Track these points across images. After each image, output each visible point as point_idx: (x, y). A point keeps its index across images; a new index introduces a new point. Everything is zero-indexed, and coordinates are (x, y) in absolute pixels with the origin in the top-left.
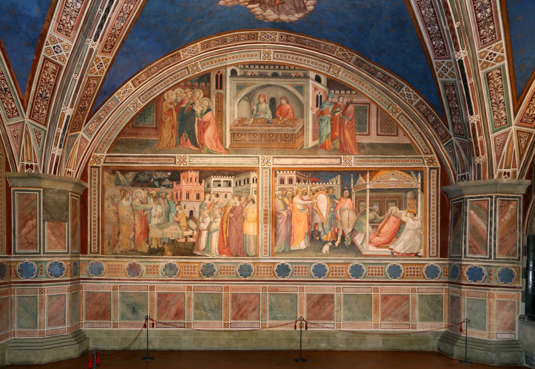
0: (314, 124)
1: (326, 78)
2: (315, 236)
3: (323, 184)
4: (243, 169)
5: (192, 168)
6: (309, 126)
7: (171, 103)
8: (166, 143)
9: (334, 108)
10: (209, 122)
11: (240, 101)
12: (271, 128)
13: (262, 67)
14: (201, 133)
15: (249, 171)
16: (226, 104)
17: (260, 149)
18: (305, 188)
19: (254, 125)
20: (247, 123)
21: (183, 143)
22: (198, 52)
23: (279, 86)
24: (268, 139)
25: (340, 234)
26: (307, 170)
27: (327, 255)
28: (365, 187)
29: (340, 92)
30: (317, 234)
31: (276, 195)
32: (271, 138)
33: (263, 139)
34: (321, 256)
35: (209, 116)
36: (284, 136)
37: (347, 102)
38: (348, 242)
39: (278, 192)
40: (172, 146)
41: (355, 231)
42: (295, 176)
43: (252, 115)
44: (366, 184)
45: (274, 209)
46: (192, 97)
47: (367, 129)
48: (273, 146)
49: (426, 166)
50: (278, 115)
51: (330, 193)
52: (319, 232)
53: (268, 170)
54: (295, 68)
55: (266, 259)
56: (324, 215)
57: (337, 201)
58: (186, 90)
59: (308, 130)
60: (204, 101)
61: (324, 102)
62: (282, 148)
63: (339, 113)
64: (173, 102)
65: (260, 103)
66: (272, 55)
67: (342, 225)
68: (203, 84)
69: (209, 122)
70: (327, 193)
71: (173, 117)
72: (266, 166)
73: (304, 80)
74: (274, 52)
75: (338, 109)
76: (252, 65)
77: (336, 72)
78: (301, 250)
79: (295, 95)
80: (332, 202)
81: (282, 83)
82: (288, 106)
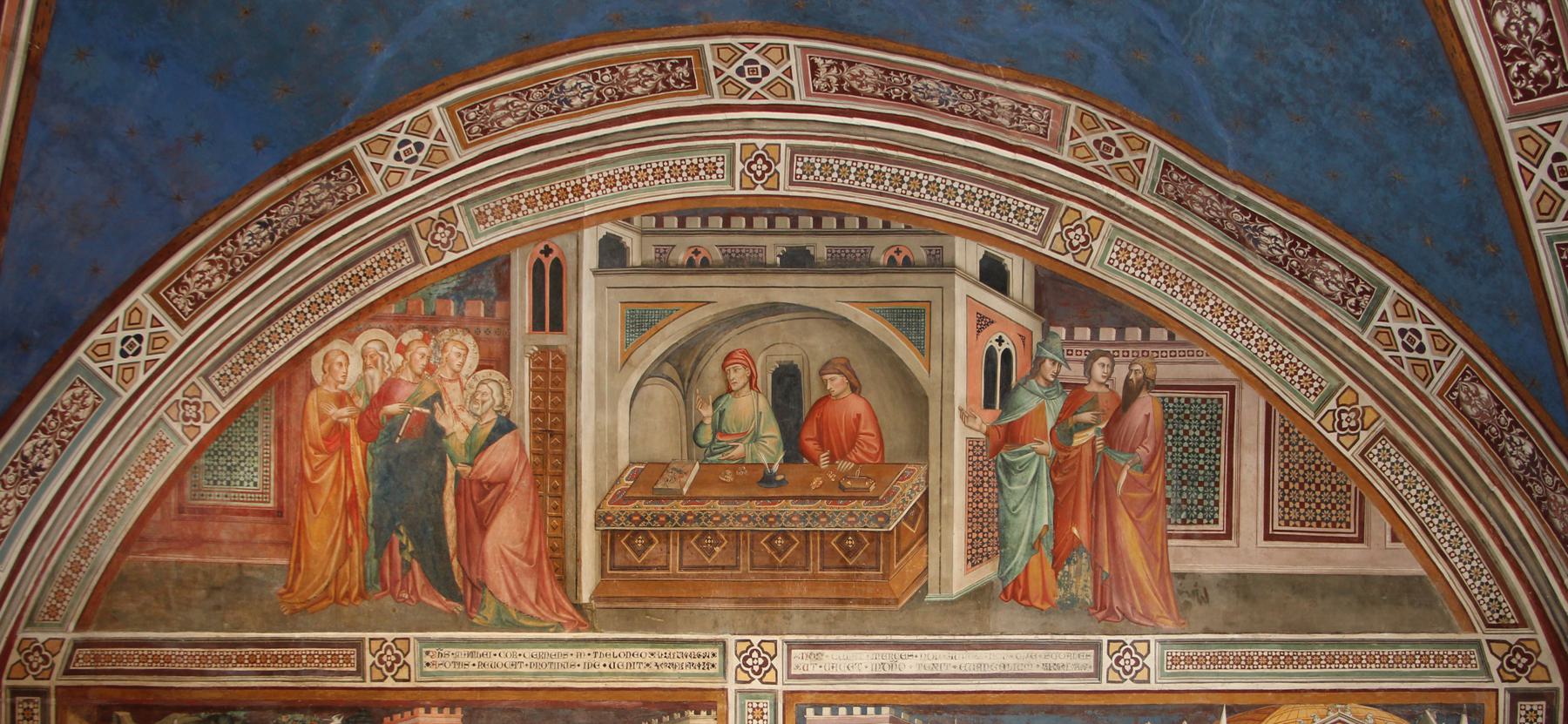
0: (975, 486)
1: (1030, 269)
4: (653, 698)
5: (432, 696)
6: (951, 495)
7: (341, 400)
8: (323, 577)
9: (1069, 409)
10: (506, 482)
11: (639, 386)
12: (776, 507)
13: (739, 223)
14: (468, 532)
15: (683, 707)
16: (577, 396)
17: (732, 606)
19: (703, 492)
20: (672, 486)
21: (394, 582)
22: (447, 158)
23: (818, 310)
24: (766, 561)
29: (1095, 335)
32: (780, 555)
33: (745, 559)
35: (502, 456)
36: (840, 543)
37: (1127, 380)
40: (348, 595)
43: (695, 450)
46: (430, 368)
47: (1222, 509)
48: (789, 591)
50: (811, 446)
53: (765, 704)
54: (886, 224)
58: (406, 339)
59: (946, 514)
60: (484, 388)
61: (1023, 383)
62: (828, 601)
63: (1091, 433)
64: (345, 393)
65: (730, 391)
66: (781, 168)
68: (477, 309)
69: (502, 484)
71: (349, 464)
72: (756, 685)
73: (928, 279)
74: (794, 150)
75: (1086, 417)
76: (695, 213)
77: (1077, 237)
79: (889, 350)
81: (831, 295)
82: (856, 405)
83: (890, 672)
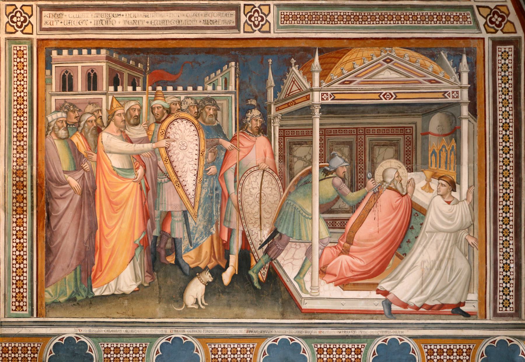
2: (163, 253)
3: (185, 89)
18: (132, 103)
25: (236, 246)
26: (139, 45)
27: (198, 310)
28: (308, 98)
30: (169, 246)
31: (49, 126)
34: (180, 314)
38: (259, 271)
39: (54, 116)
41: (281, 235)
42: (104, 65)
44: (312, 90)
45: (43, 169)
49: (484, 35)
51: (207, 120)
52: (174, 239)
55: (20, 325)
56: (190, 187)
57: (227, 145)
67: (241, 218)
70: (197, 118)
78: (124, 295)
80: (215, 147)
83: (106, 26)
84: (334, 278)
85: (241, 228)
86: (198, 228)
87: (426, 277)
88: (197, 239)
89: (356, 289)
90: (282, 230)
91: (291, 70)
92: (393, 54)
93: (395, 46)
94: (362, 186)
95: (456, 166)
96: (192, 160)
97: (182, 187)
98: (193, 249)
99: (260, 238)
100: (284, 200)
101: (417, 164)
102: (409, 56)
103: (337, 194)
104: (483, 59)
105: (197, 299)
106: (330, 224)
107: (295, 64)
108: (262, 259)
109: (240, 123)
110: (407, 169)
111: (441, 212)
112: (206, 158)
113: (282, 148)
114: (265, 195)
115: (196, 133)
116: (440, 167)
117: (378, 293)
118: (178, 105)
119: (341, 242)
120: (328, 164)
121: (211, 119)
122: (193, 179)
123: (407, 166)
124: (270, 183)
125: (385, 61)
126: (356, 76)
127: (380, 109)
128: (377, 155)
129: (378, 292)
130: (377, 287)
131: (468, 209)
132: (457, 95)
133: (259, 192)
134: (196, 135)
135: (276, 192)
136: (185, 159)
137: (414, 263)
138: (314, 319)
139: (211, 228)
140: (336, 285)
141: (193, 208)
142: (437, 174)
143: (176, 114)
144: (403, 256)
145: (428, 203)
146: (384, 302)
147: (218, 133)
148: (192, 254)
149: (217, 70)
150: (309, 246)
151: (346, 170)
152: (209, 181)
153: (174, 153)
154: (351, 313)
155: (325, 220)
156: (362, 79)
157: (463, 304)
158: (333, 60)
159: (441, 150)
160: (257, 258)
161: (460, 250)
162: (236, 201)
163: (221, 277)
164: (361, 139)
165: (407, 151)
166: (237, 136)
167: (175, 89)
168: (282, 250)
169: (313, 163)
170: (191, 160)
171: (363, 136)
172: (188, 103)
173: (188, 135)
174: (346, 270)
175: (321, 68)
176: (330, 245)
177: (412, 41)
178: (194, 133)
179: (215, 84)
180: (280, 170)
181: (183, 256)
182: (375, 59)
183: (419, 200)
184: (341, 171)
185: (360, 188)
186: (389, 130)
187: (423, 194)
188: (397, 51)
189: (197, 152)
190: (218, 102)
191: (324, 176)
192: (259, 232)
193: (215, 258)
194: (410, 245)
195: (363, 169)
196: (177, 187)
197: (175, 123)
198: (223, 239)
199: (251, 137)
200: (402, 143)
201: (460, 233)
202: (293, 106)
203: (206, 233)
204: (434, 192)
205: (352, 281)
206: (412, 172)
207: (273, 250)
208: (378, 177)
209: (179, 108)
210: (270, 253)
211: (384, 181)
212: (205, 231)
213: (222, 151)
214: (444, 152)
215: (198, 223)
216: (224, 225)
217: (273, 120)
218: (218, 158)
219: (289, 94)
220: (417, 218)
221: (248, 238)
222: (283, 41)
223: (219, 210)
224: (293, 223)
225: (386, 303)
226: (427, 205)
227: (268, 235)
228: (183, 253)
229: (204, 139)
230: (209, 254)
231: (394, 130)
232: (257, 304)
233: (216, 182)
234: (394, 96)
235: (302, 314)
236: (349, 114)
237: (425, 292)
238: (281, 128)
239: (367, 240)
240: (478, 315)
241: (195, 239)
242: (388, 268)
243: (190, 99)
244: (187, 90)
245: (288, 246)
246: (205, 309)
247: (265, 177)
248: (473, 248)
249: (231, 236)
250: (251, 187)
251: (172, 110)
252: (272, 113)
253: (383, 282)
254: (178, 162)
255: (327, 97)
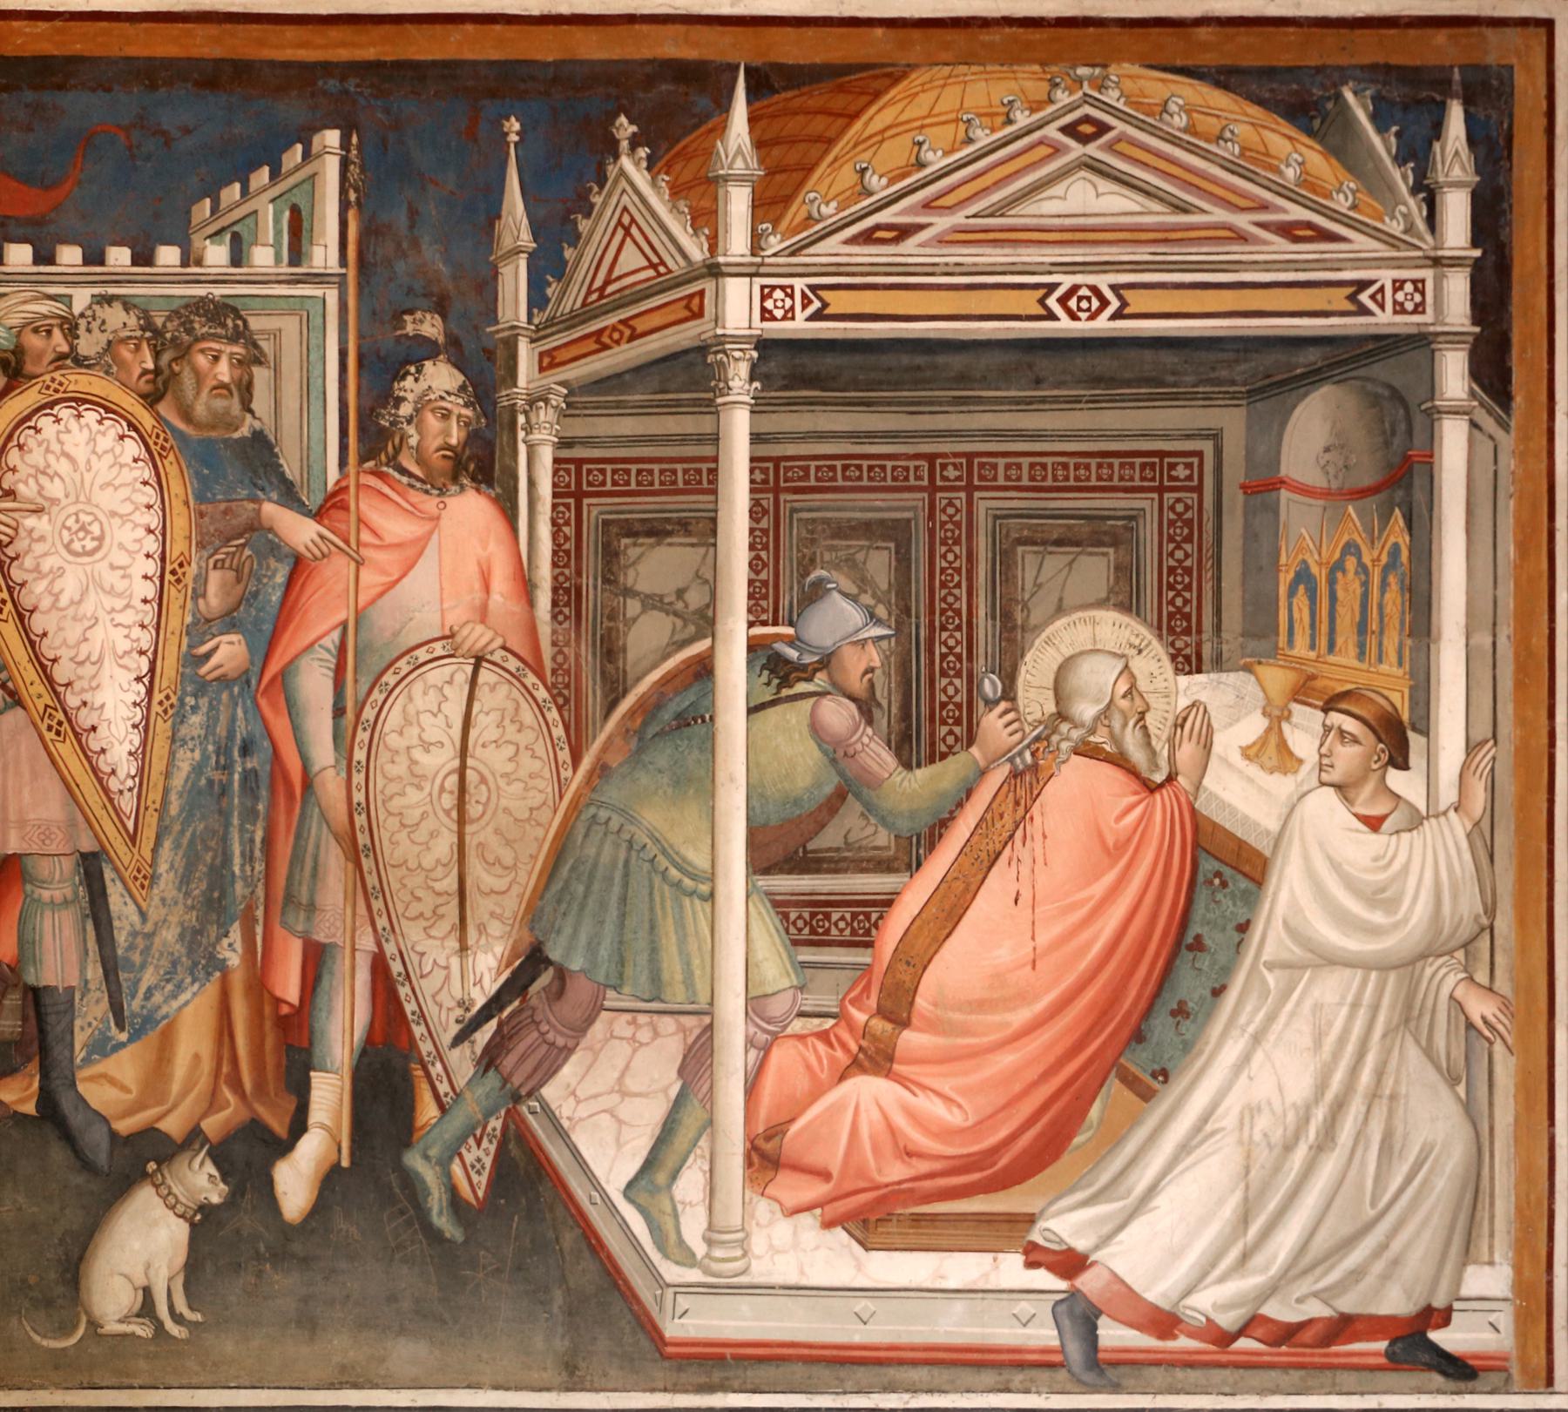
3: (94, 257)
28: (694, 310)
38: (455, 1152)
41: (562, 975)
44: (714, 271)
51: (200, 410)
52: (36, 995)
57: (301, 532)
70: (151, 399)
84: (819, 1190)
85: (367, 943)
86: (157, 940)
87: (1266, 1187)
88: (149, 995)
89: (925, 1241)
90: (570, 949)
91: (612, 171)
92: (1111, 97)
93: (1120, 60)
94: (957, 740)
95: (1409, 642)
96: (128, 606)
97: (76, 734)
98: (130, 1040)
99: (457, 992)
100: (575, 806)
101: (1224, 635)
102: (1188, 110)
103: (836, 780)
104: (1544, 121)
105: (147, 1292)
106: (800, 923)
107: (635, 143)
108: (468, 1095)
109: (362, 429)
110: (1173, 658)
111: (1335, 866)
112: (195, 598)
113: (567, 552)
114: (483, 780)
115: (147, 473)
116: (1331, 646)
117: (1030, 1265)
118: (57, 333)
119: (853, 1011)
120: (790, 631)
121: (219, 404)
122: (132, 698)
123: (1173, 644)
124: (507, 722)
125: (1068, 130)
126: (927, 206)
127: (1044, 364)
128: (1029, 585)
129: (1035, 1257)
130: (1028, 1231)
131: (1467, 856)
132: (1418, 298)
133: (457, 763)
134: (145, 483)
135: (535, 765)
136: (92, 596)
137: (1205, 1118)
138: (723, 1387)
139: (218, 939)
140: (828, 1225)
141: (133, 838)
142: (1319, 684)
143: (47, 378)
144: (1155, 1084)
145: (1273, 825)
146: (1062, 1308)
147: (255, 472)
148: (126, 1066)
149: (255, 166)
150: (697, 1032)
151: (877, 663)
152: (211, 707)
153: (37, 569)
154: (901, 1362)
155: (776, 904)
156: (959, 218)
157: (1443, 1317)
158: (819, 124)
159: (1338, 566)
160: (443, 1088)
161: (1428, 1052)
162: (342, 808)
163: (270, 1183)
164: (951, 511)
165: (1171, 570)
166: (347, 488)
167: (44, 257)
168: (568, 1051)
169: (719, 627)
170: (119, 603)
171: (963, 495)
172: (109, 327)
173: (109, 484)
174: (876, 1149)
175: (761, 161)
176: (798, 1026)
177: (1203, 33)
178: (137, 473)
179: (245, 235)
180: (560, 659)
181: (80, 1075)
182: (1022, 119)
183: (1233, 811)
184: (857, 665)
185: (944, 749)
186: (1087, 467)
187: (1250, 780)
188: (1128, 85)
189: (151, 567)
190: (255, 323)
191: (772, 689)
192: (455, 962)
193: (237, 1086)
194: (1187, 1026)
195: (959, 657)
196: (49, 736)
197: (45, 422)
198: (279, 993)
199: (415, 496)
200: (1149, 532)
201: (1429, 971)
202: (625, 346)
203: (195, 964)
204: (1305, 769)
205: (905, 1206)
206: (1199, 671)
207: (522, 1047)
208: (1032, 694)
209: (65, 348)
210: (508, 1062)
211: (1061, 716)
212: (190, 952)
213: (273, 563)
214: (1351, 575)
215: (154, 914)
216: (284, 924)
217: (526, 413)
218: (255, 595)
219: (602, 289)
220: (1219, 896)
221: (404, 991)
222: (578, 32)
223: (258, 853)
224: (623, 916)
225: (1071, 1313)
226: (1268, 833)
227: (499, 974)
228: (78, 1061)
229: (187, 503)
230: (207, 1066)
231: (1111, 466)
232: (447, 1316)
233: (245, 713)
234: (1115, 304)
235: (666, 1364)
236: (897, 386)
237: (1258, 1260)
238: (565, 454)
239: (981, 1005)
240: (1515, 1371)
241: (141, 994)
242: (1077, 1140)
243: (118, 306)
244: (102, 263)
245: (598, 1029)
246: (187, 1342)
247: (482, 693)
248: (1491, 1043)
249: (317, 979)
250: (415, 741)
251: (28, 359)
252: (522, 381)
253: (1055, 1208)
254: (54, 615)
255: (788, 303)
